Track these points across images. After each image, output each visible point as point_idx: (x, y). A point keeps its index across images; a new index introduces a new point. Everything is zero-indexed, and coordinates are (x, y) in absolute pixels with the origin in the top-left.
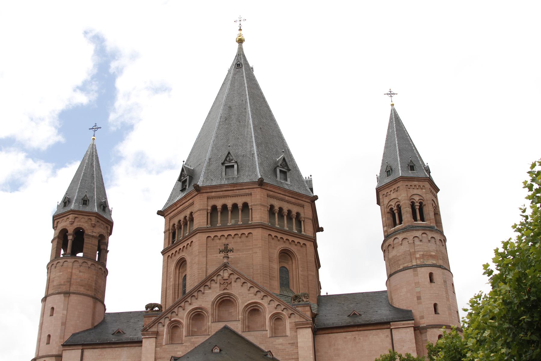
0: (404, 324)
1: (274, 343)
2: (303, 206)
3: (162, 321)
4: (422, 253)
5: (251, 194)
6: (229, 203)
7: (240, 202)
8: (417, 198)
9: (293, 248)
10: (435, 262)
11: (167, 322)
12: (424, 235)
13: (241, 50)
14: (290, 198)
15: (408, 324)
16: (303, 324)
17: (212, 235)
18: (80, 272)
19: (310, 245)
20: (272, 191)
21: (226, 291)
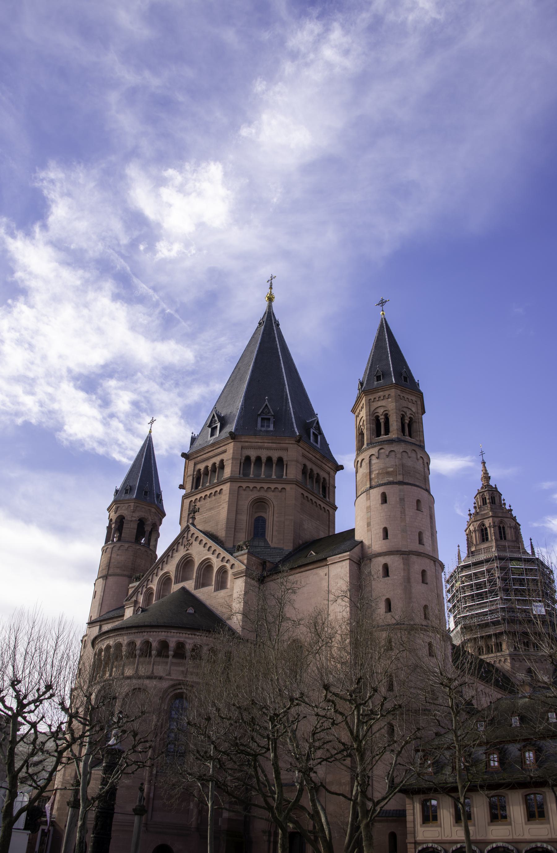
0: (340, 558)
1: (217, 597)
2: (287, 449)
3: (140, 590)
4: (377, 472)
5: (225, 452)
6: (210, 464)
7: (217, 460)
8: (381, 411)
9: (270, 495)
10: (391, 479)
11: (144, 590)
12: (382, 451)
13: (270, 307)
14: (270, 444)
15: (344, 557)
16: (239, 574)
17: (193, 499)
18: (117, 555)
19: (291, 489)
20: (247, 442)
21: (188, 552)
